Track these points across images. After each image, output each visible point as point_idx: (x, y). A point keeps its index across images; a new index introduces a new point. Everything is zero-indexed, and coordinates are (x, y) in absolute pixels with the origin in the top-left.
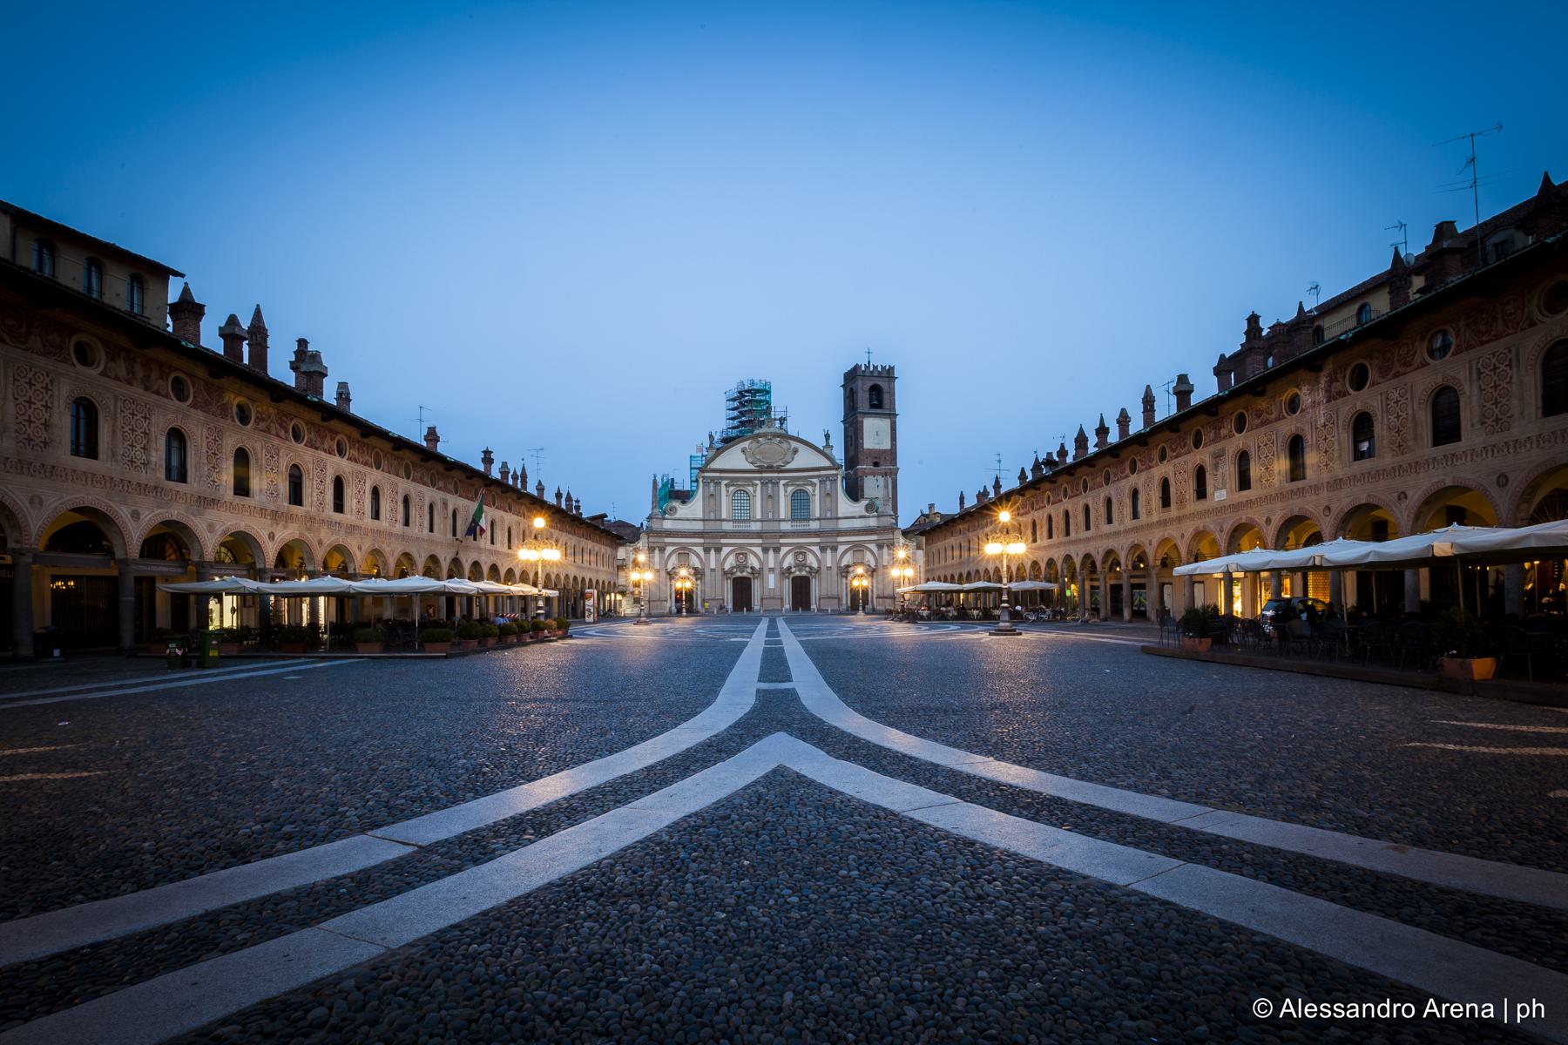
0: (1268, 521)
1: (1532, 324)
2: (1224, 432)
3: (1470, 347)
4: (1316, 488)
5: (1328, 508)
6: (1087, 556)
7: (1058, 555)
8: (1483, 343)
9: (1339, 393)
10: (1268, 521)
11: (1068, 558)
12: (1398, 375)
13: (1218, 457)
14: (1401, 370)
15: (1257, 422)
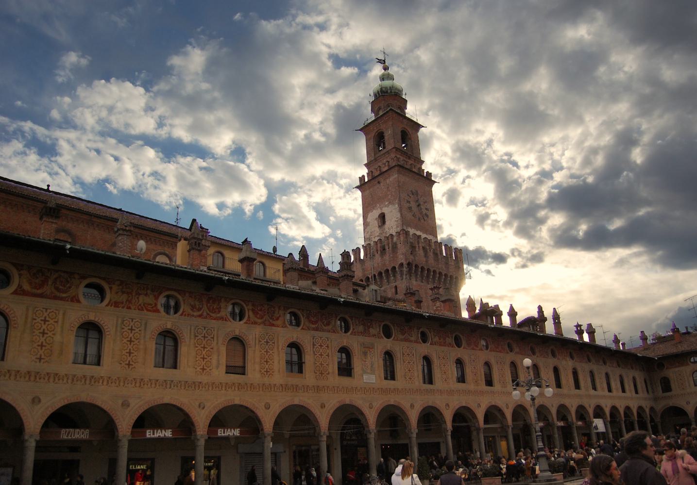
0: (412, 406)
1: (508, 353)
2: (372, 331)
3: (494, 351)
4: (441, 392)
5: (447, 405)
6: (628, 408)
7: (646, 405)
8: (497, 351)
9: (450, 344)
10: (412, 406)
11: (628, 408)
12: (473, 349)
13: (367, 349)
14: (475, 348)
15: (401, 337)
